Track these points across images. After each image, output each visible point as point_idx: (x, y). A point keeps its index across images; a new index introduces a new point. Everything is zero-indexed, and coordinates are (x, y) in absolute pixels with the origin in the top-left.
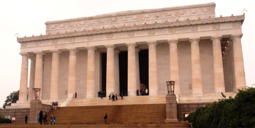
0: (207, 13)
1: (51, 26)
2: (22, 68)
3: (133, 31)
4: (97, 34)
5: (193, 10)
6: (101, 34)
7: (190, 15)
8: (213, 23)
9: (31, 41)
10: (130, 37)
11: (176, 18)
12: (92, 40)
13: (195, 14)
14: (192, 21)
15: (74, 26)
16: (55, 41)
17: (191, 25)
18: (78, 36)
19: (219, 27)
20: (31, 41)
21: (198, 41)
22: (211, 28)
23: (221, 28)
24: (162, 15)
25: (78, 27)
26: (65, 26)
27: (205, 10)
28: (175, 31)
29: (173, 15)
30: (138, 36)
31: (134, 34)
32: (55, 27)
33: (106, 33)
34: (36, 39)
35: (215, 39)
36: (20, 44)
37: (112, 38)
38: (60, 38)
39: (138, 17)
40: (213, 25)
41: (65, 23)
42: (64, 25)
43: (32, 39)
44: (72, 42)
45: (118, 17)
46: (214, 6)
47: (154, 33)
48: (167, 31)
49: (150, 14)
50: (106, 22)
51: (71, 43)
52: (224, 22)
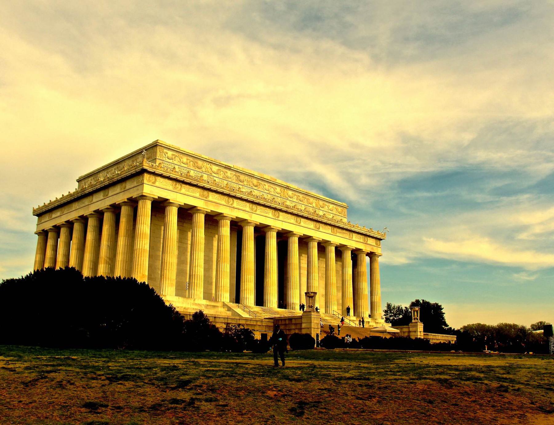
1: (167, 153)
3: (302, 217)
12: (256, 211)
15: (204, 169)
16: (206, 193)
20: (169, 178)
22: (361, 238)
29: (314, 205)
33: (275, 209)
34: (179, 178)
37: (278, 217)
41: (189, 158)
42: (187, 159)
47: (319, 228)
48: (329, 229)
50: (245, 183)
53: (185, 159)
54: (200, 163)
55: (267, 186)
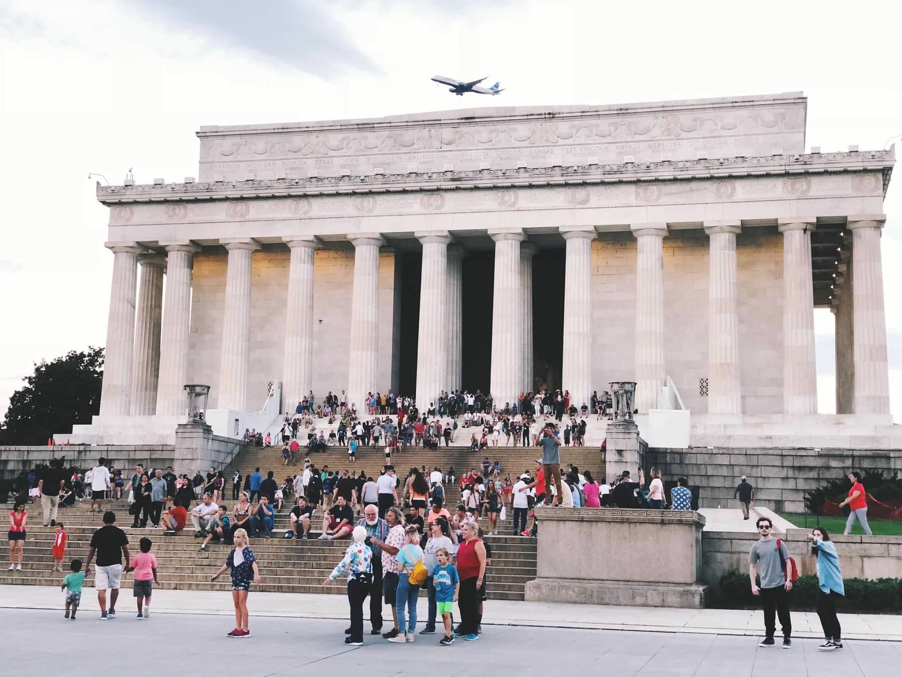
0: (775, 130)
2: (113, 296)
3: (513, 187)
4: (388, 192)
5: (729, 116)
6: (404, 192)
7: (716, 134)
8: (787, 174)
9: (150, 202)
10: (504, 208)
11: (665, 142)
13: (732, 132)
14: (717, 163)
15: (303, 152)
16: (241, 207)
17: (712, 178)
18: (321, 195)
19: (808, 189)
21: (733, 232)
22: (778, 187)
23: (813, 193)
24: (616, 129)
25: (319, 155)
26: (272, 147)
27: (768, 114)
28: (658, 198)
29: (656, 132)
30: (532, 205)
31: (517, 197)
32: (235, 148)
33: (421, 191)
35: (793, 229)
36: (107, 210)
37: (440, 207)
38: (258, 198)
39: (534, 133)
40: (788, 181)
43: (153, 196)
44: (300, 214)
45: (464, 129)
46: (802, 105)
47: (587, 201)
49: (576, 122)
51: (298, 216)
52: (826, 173)
53: (260, 144)
54: (298, 141)
55: (482, 132)
